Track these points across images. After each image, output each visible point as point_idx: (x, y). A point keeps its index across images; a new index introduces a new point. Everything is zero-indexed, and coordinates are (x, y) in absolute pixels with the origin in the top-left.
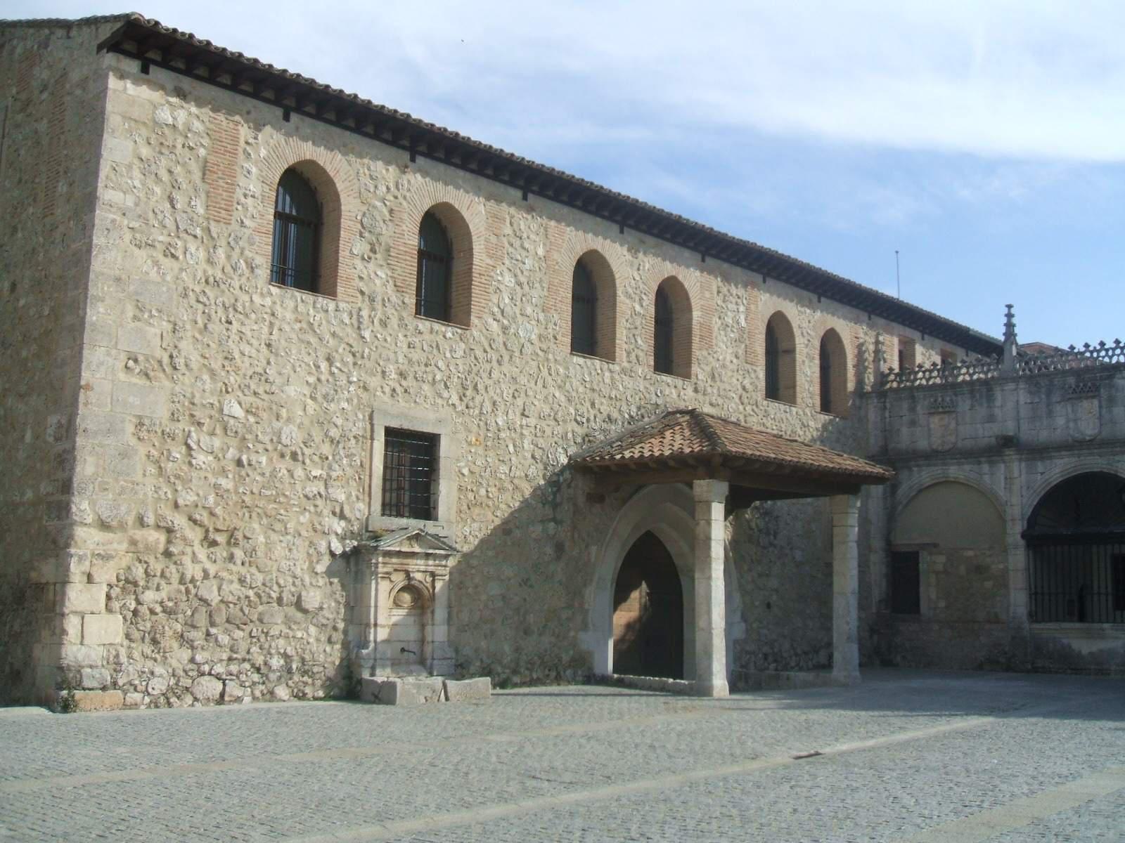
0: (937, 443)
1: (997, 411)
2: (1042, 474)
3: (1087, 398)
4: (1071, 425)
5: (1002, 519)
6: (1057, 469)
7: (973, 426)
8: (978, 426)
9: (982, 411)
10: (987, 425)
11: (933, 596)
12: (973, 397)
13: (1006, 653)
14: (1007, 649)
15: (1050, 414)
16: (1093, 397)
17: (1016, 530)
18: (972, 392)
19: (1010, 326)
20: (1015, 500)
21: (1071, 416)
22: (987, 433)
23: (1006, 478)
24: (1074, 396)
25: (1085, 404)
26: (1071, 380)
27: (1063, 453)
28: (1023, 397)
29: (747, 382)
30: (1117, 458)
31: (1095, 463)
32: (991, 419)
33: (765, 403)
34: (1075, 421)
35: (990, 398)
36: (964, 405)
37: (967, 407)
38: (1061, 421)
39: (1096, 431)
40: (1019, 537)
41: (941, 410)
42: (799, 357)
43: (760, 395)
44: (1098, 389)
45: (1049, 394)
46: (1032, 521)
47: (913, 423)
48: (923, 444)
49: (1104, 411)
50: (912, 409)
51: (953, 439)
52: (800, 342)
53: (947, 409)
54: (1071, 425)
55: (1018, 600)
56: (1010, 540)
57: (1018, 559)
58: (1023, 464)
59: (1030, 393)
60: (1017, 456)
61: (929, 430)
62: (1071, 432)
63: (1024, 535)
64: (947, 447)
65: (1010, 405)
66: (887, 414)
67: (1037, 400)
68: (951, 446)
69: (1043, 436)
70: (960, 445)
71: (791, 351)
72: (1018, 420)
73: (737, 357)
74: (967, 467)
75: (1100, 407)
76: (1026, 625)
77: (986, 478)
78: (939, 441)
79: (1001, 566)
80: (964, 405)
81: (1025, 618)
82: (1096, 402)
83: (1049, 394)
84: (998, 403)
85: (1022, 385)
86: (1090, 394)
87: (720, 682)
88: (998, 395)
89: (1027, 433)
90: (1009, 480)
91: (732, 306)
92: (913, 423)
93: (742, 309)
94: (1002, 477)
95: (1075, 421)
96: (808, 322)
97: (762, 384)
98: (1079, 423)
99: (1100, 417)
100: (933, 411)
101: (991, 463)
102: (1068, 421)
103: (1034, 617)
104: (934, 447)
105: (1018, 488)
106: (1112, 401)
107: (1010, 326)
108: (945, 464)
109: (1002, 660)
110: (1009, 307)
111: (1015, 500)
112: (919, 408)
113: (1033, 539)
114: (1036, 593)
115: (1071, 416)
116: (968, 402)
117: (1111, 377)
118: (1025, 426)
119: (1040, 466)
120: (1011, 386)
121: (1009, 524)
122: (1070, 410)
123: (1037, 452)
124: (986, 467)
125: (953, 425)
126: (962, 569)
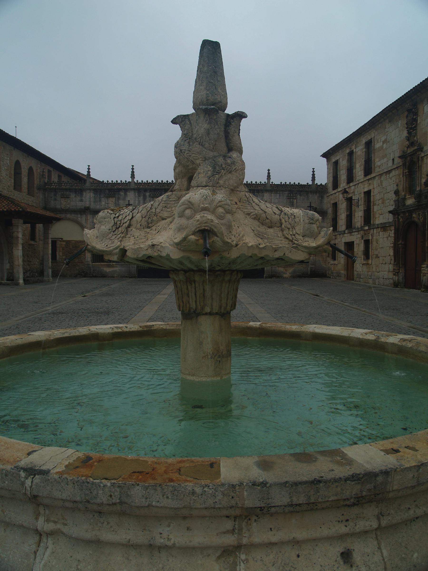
1: (84, 198)
3: (112, 197)
4: (106, 205)
8: (78, 202)
9: (79, 198)
10: (80, 202)
11: (61, 254)
15: (100, 201)
19: (89, 172)
21: (106, 202)
22: (80, 205)
25: (111, 199)
28: (92, 195)
29: (9, 184)
32: (81, 200)
33: (14, 191)
34: (108, 204)
37: (74, 196)
38: (103, 203)
42: (23, 176)
43: (12, 188)
47: (55, 200)
48: (58, 207)
51: (68, 206)
52: (23, 170)
59: (94, 194)
71: (20, 173)
72: (90, 201)
73: (7, 175)
74: (73, 215)
76: (91, 264)
77: (79, 219)
82: (114, 198)
84: (84, 196)
87: (21, 281)
88: (84, 194)
91: (6, 158)
92: (55, 200)
93: (8, 159)
95: (108, 204)
96: (26, 163)
97: (13, 185)
99: (115, 203)
101: (81, 214)
102: (105, 203)
106: (119, 199)
107: (89, 172)
109: (83, 274)
112: (57, 195)
118: (92, 203)
120: (89, 191)
124: (79, 216)
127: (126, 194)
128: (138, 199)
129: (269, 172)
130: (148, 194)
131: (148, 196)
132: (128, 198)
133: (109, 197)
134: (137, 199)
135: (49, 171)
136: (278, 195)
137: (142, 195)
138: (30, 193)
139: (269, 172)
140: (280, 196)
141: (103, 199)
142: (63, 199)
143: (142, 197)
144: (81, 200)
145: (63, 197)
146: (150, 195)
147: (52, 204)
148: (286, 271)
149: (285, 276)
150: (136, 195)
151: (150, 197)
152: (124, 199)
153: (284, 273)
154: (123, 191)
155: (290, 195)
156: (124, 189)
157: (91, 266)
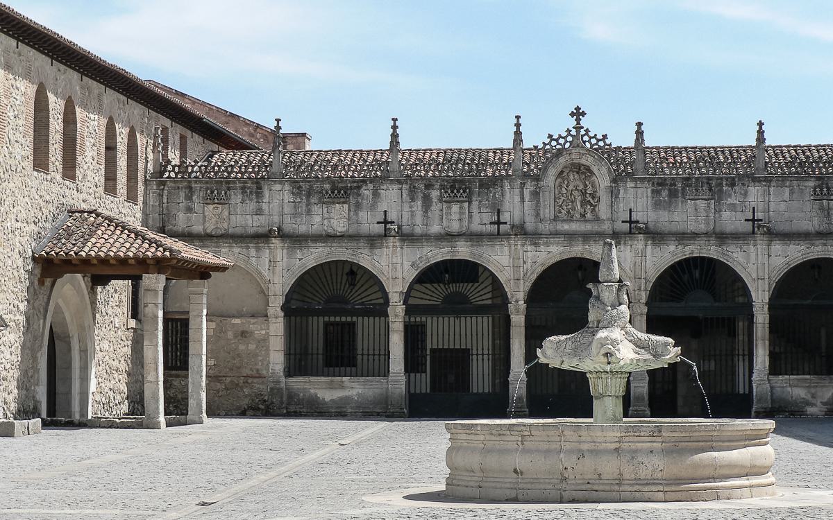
0: (210, 228)
1: (265, 207)
2: (300, 259)
4: (326, 222)
5: (264, 295)
6: (314, 256)
7: (242, 215)
9: (251, 206)
10: (255, 217)
12: (244, 192)
13: (265, 401)
14: (266, 398)
15: (309, 212)
16: (344, 203)
17: (276, 303)
18: (243, 189)
20: (277, 279)
22: (255, 224)
23: (270, 261)
24: (330, 200)
26: (327, 186)
27: (318, 244)
28: (288, 197)
30: (359, 251)
31: (341, 253)
32: (259, 212)
35: (259, 193)
36: (236, 198)
38: (317, 219)
39: (345, 229)
40: (279, 309)
41: (216, 201)
44: (348, 197)
45: (309, 195)
46: (289, 298)
48: (198, 229)
49: (352, 213)
50: (189, 198)
51: (225, 225)
53: (222, 201)
54: (326, 222)
55: (277, 360)
56: (271, 311)
57: (276, 328)
58: (285, 251)
59: (293, 193)
60: (281, 245)
61: (205, 217)
62: (325, 228)
63: (284, 308)
64: (219, 232)
65: (275, 204)
66: (165, 201)
67: (299, 200)
68: (224, 232)
69: (303, 229)
70: (231, 231)
75: (349, 210)
76: (283, 379)
78: (213, 227)
79: (264, 332)
80: (236, 198)
81: (282, 374)
82: (346, 206)
83: (309, 195)
85: (287, 187)
86: (342, 200)
87: (162, 419)
88: (266, 193)
89: (290, 225)
90: (272, 262)
92: (189, 210)
94: (267, 260)
98: (332, 221)
99: (349, 219)
100: (209, 202)
101: (258, 249)
102: (323, 219)
103: (289, 373)
104: (208, 231)
105: (280, 269)
106: (358, 206)
108: (217, 247)
109: (261, 406)
110: (278, 120)
111: (277, 279)
113: (287, 309)
114: (290, 354)
115: (326, 215)
116: (240, 197)
117: (359, 188)
118: (287, 220)
119: (299, 254)
120: (278, 187)
121: (271, 299)
122: (325, 210)
123: (296, 240)
124: (253, 252)
125: (226, 213)
126: (230, 335)
127: (376, 194)
128: (411, 207)
129: (760, 128)
130: (435, 194)
131: (435, 200)
132: (383, 206)
133: (334, 203)
134: (406, 208)
135: (165, 130)
136: (787, 190)
137: (420, 195)
138: (132, 197)
139: (760, 128)
140: (792, 192)
141: (316, 208)
142: (211, 207)
143: (419, 203)
144: (259, 212)
145: (210, 199)
146: (441, 196)
147: (181, 221)
148: (813, 396)
149: (810, 410)
150: (404, 196)
151: (441, 201)
152: (373, 208)
153: (808, 404)
154: (370, 186)
155: (821, 190)
156: (372, 180)
157: (283, 385)
